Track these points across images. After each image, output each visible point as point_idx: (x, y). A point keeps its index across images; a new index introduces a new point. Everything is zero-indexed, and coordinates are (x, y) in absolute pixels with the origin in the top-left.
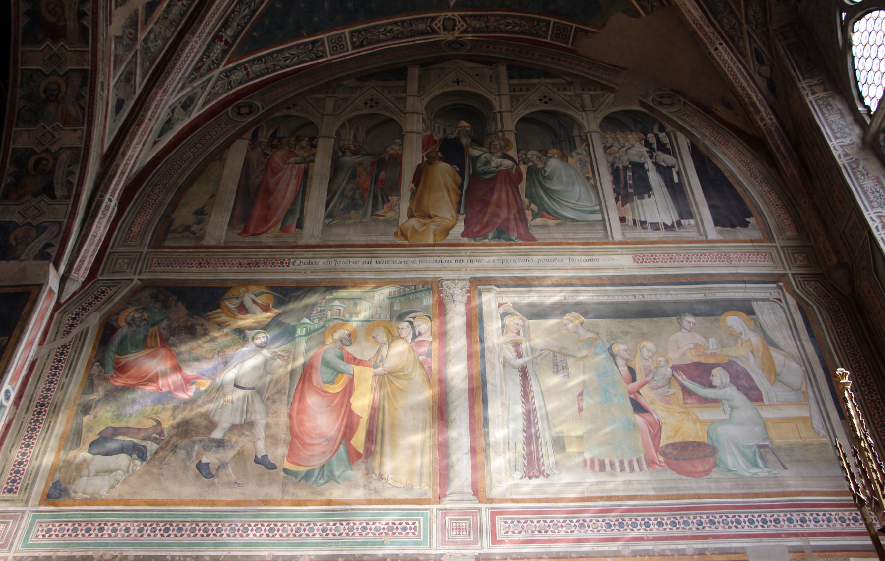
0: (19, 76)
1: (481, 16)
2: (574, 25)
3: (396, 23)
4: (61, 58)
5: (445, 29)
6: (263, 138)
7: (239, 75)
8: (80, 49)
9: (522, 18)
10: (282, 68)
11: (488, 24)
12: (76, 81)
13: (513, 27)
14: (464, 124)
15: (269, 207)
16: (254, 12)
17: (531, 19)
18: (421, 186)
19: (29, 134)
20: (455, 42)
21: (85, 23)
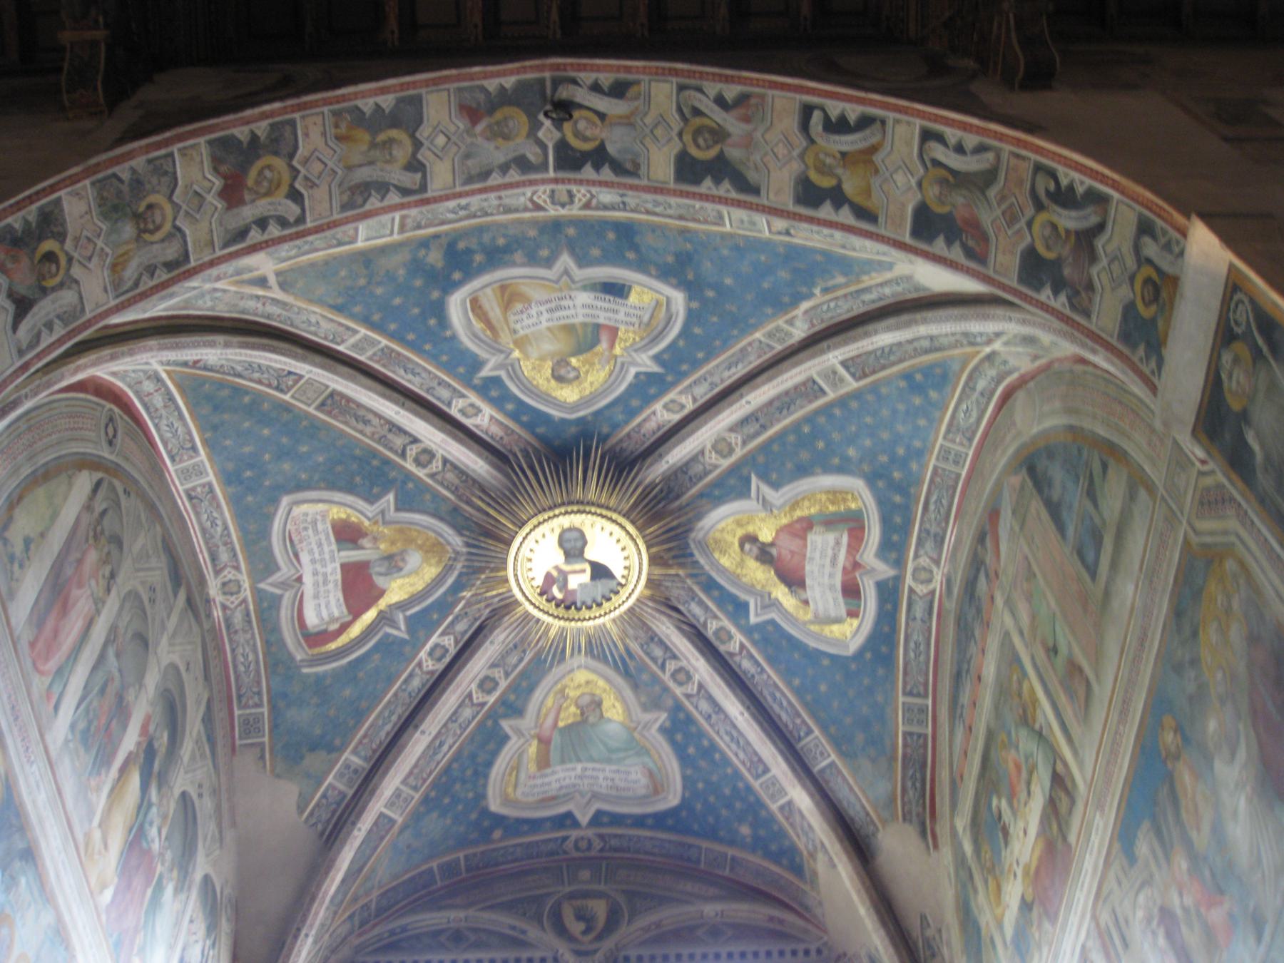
0: (163, 152)
1: (250, 622)
2: (266, 739)
3: (226, 528)
4: (198, 211)
5: (224, 584)
6: (99, 506)
7: (148, 386)
8: (215, 238)
9: (258, 672)
10: (156, 426)
11: (241, 632)
12: (171, 252)
13: (242, 663)
14: (166, 735)
15: (56, 633)
16: (240, 376)
17: (259, 683)
18: (120, 783)
19: (86, 213)
20: (208, 601)
21: (252, 233)
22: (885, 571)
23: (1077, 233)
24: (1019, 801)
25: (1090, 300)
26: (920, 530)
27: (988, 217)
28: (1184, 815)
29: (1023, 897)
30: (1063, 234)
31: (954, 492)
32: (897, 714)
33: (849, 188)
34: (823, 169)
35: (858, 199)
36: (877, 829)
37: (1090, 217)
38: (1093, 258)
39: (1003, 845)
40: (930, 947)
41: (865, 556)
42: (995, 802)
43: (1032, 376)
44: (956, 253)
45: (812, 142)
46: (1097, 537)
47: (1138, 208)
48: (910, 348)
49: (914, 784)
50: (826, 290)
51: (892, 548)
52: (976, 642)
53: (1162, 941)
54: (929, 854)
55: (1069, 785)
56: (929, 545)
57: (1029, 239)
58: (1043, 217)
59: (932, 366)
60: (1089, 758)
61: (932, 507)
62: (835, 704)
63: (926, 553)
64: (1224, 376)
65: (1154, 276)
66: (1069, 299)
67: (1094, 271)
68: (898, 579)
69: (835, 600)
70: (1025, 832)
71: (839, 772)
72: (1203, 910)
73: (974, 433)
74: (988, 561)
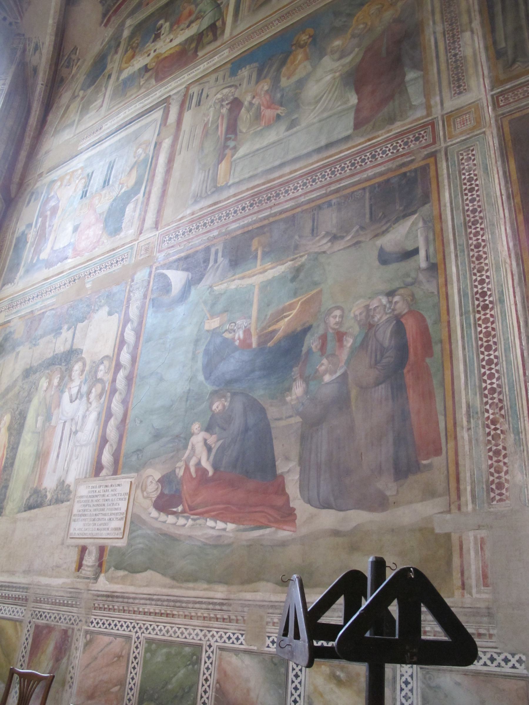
24: (178, 27)
28: (284, 70)
29: (146, 65)
39: (151, 40)
40: (69, 63)
42: (161, 22)
53: (224, 111)
55: (219, 32)
60: (242, 26)
70: (171, 41)
72: (262, 108)
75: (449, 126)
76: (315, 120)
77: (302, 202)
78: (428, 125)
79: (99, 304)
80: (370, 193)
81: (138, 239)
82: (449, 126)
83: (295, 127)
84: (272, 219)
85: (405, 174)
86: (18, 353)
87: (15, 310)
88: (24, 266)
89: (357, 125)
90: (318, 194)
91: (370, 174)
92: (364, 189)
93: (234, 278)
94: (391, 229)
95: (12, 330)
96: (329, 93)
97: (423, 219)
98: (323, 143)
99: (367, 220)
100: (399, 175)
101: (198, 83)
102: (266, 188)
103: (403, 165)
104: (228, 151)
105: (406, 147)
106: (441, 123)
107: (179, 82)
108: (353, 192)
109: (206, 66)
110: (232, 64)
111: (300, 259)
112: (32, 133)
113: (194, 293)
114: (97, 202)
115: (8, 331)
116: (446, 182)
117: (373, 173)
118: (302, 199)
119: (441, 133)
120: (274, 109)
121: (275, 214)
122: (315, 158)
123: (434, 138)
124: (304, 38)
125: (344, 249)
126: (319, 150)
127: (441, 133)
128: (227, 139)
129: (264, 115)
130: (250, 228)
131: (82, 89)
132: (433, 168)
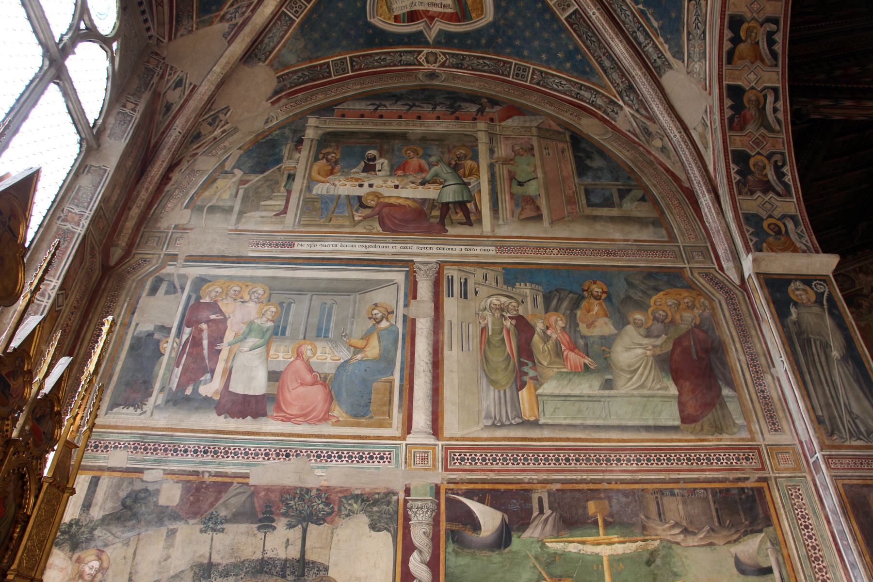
22: (431, 35)
23: (768, 181)
25: (746, 193)
26: (463, 55)
27: (750, 128)
30: (764, 173)
31: (495, 74)
32: (337, 56)
33: (742, 47)
34: (749, 31)
35: (737, 53)
36: (264, 62)
37: (780, 189)
38: (765, 192)
40: (214, 120)
41: (437, 23)
43: (614, 128)
44: (728, 113)
45: (761, 26)
46: (608, 203)
47: (798, 213)
48: (599, 53)
49: (301, 77)
50: (642, 13)
51: (447, 40)
52: (434, 108)
53: (508, 323)
54: (267, 100)
56: (454, 61)
57: (753, 154)
58: (766, 162)
59: (590, 65)
61: (481, 61)
62: (332, 15)
63: (447, 59)
64: (792, 284)
65: (783, 230)
66: (739, 180)
67: (759, 194)
68: (427, 44)
69: (406, 7)
70: (396, 187)
71: (289, 28)
73: (544, 87)
74: (487, 110)
75: (773, 458)
76: (636, 392)
77: (640, 479)
78: (755, 449)
79: (349, 508)
80: (713, 496)
81: (405, 439)
82: (773, 458)
83: (612, 389)
84: (605, 486)
85: (743, 489)
86: (172, 533)
87: (149, 457)
88: (162, 390)
89: (685, 419)
90: (657, 477)
91: (708, 476)
92: (705, 489)
93: (571, 539)
94: (741, 540)
95: (151, 488)
96: (645, 368)
97: (770, 541)
98: (651, 423)
99: (717, 524)
100: (738, 488)
101: (456, 268)
102: (593, 446)
103: (739, 480)
104: (525, 378)
105: (739, 463)
106: (765, 451)
107: (423, 251)
108: (695, 489)
109: (463, 252)
110: (504, 269)
111: (652, 542)
112: (151, 187)
113: (517, 543)
114: (309, 353)
115: (138, 486)
116: (782, 510)
117: (711, 476)
118: (640, 476)
119: (768, 463)
120: (580, 355)
121: (609, 482)
122: (644, 435)
123: (762, 464)
124: (596, 289)
125: (698, 546)
126: (648, 428)
127: (768, 463)
128: (521, 364)
129: (567, 355)
130: (581, 486)
131: (237, 166)
132: (767, 493)
